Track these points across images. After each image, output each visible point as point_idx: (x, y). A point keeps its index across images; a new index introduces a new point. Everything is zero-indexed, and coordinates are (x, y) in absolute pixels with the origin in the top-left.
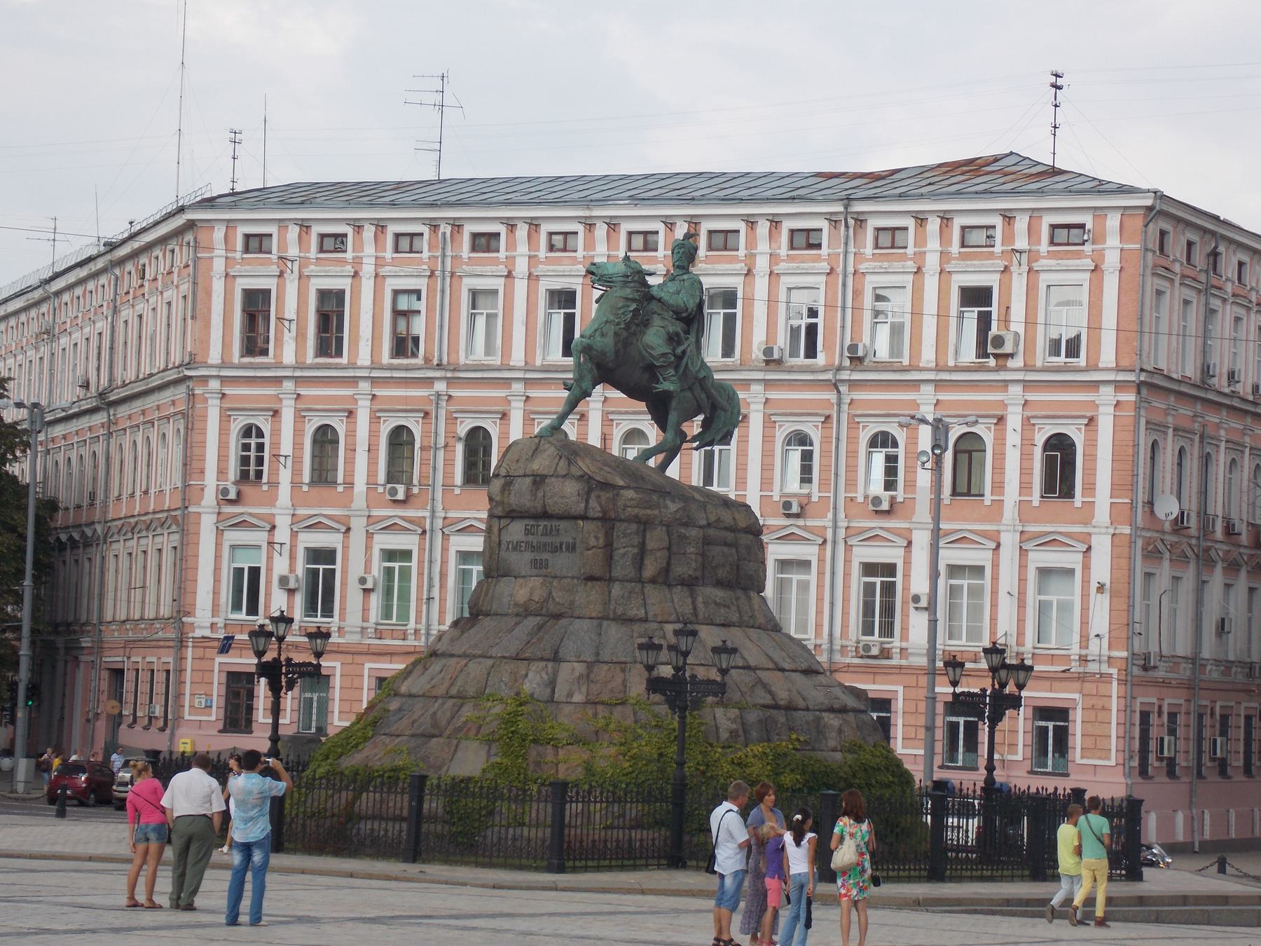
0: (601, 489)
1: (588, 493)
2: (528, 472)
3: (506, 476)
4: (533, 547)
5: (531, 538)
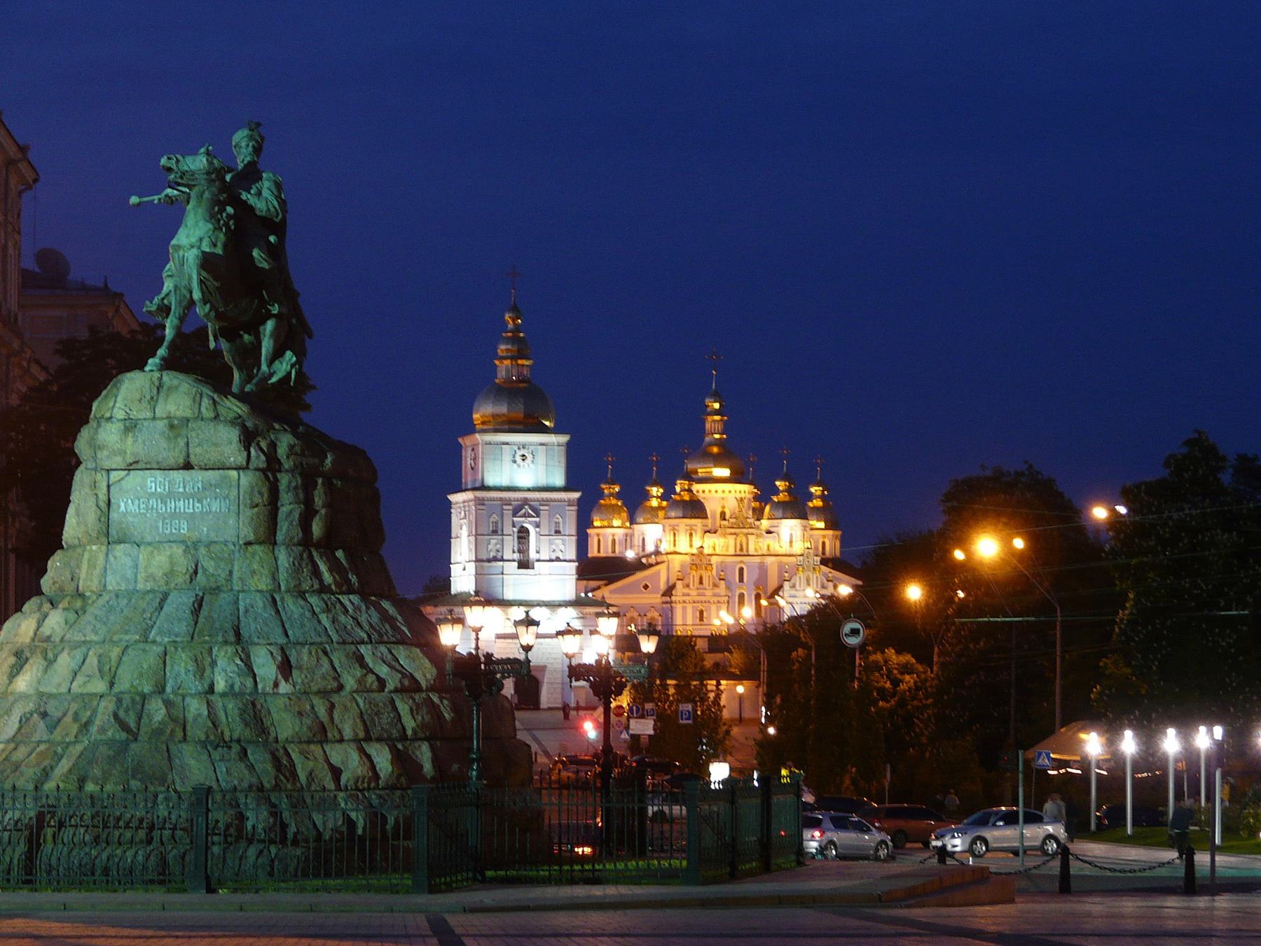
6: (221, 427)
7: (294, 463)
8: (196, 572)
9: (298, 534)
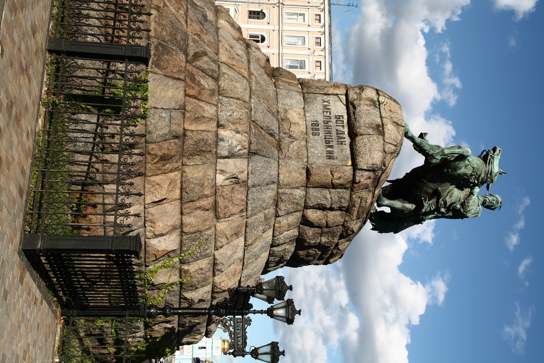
0: (374, 179)
1: (374, 171)
2: (384, 120)
3: (379, 101)
4: (328, 122)
5: (334, 120)
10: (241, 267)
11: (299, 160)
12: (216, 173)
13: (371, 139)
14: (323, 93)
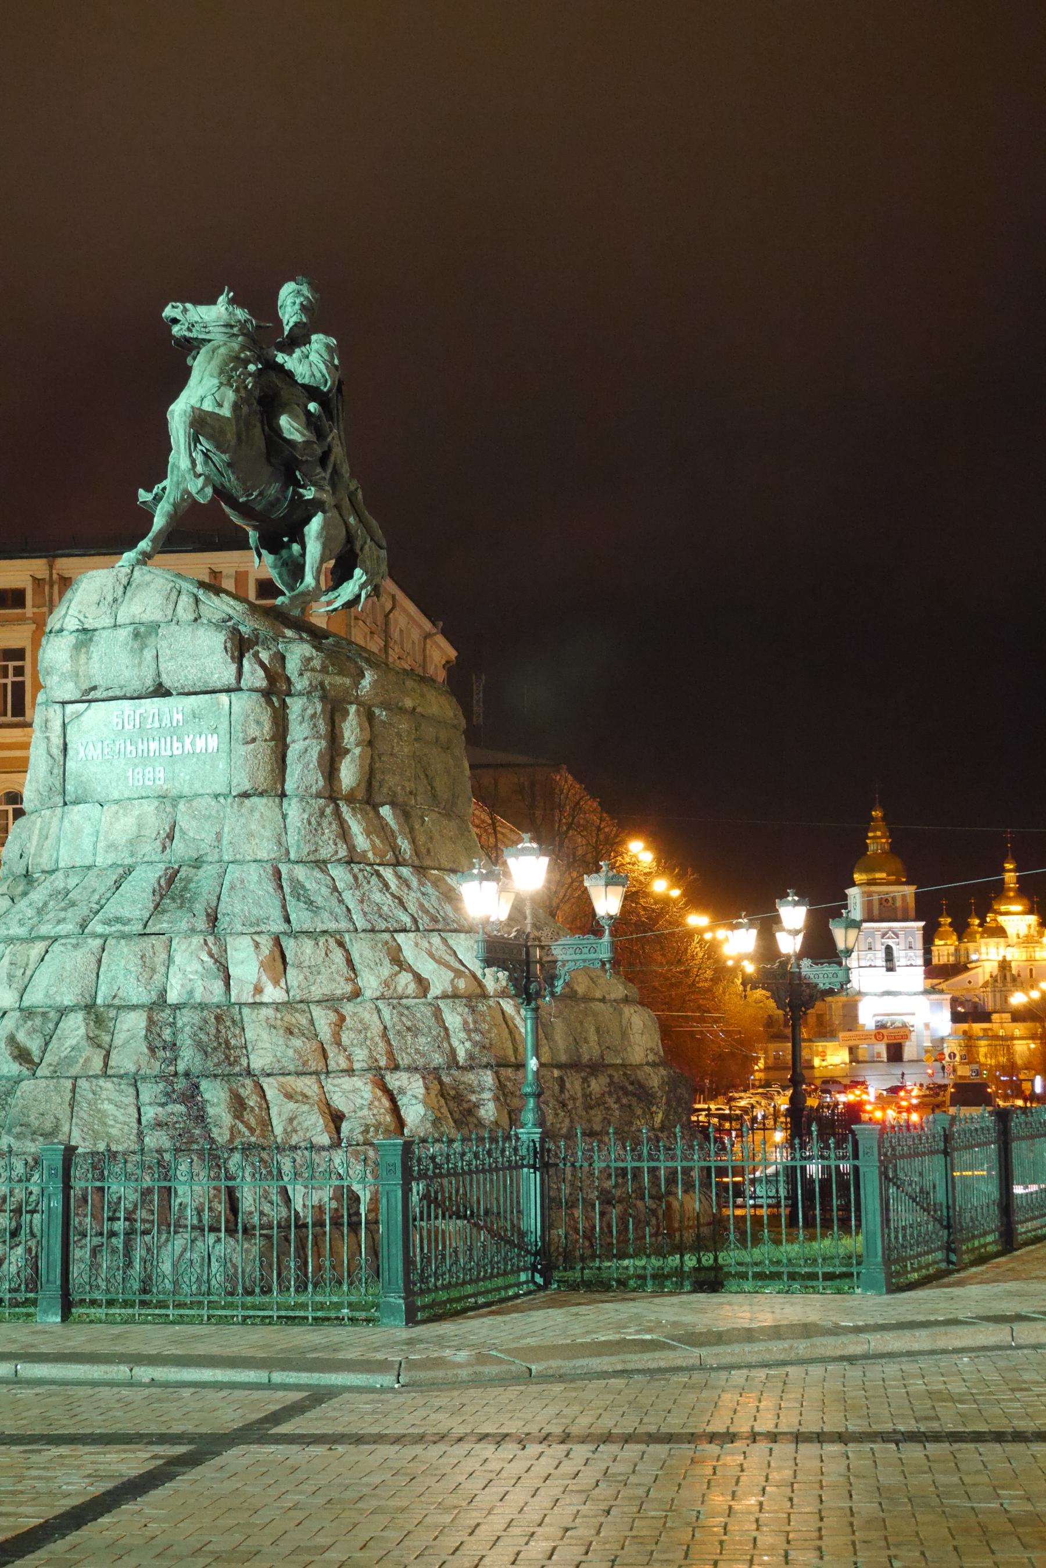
6: (201, 632)
7: (311, 684)
8: (171, 837)
9: (318, 782)
10: (462, 935)
11: (222, 815)
12: (261, 1004)
13: (168, 652)
14: (62, 758)
